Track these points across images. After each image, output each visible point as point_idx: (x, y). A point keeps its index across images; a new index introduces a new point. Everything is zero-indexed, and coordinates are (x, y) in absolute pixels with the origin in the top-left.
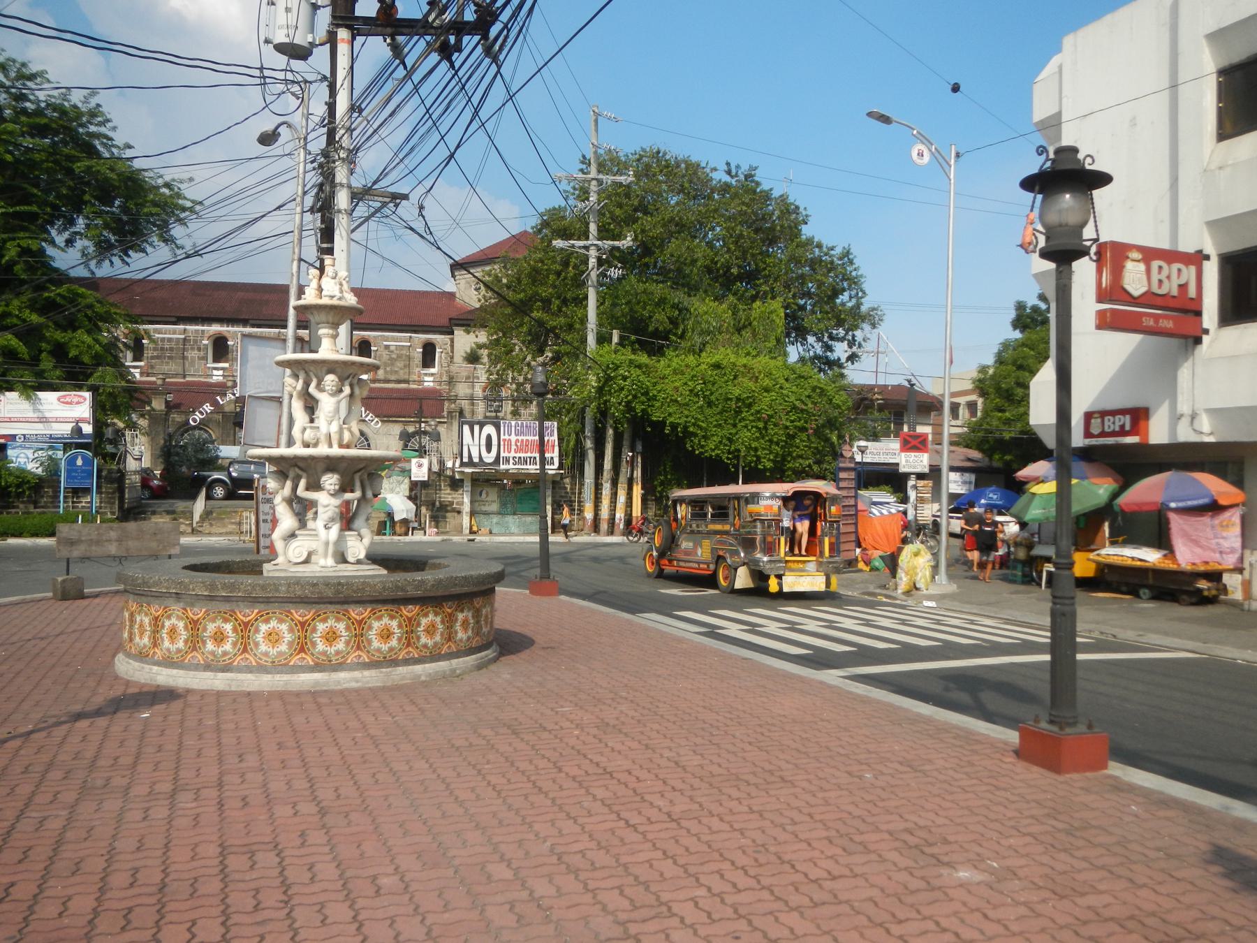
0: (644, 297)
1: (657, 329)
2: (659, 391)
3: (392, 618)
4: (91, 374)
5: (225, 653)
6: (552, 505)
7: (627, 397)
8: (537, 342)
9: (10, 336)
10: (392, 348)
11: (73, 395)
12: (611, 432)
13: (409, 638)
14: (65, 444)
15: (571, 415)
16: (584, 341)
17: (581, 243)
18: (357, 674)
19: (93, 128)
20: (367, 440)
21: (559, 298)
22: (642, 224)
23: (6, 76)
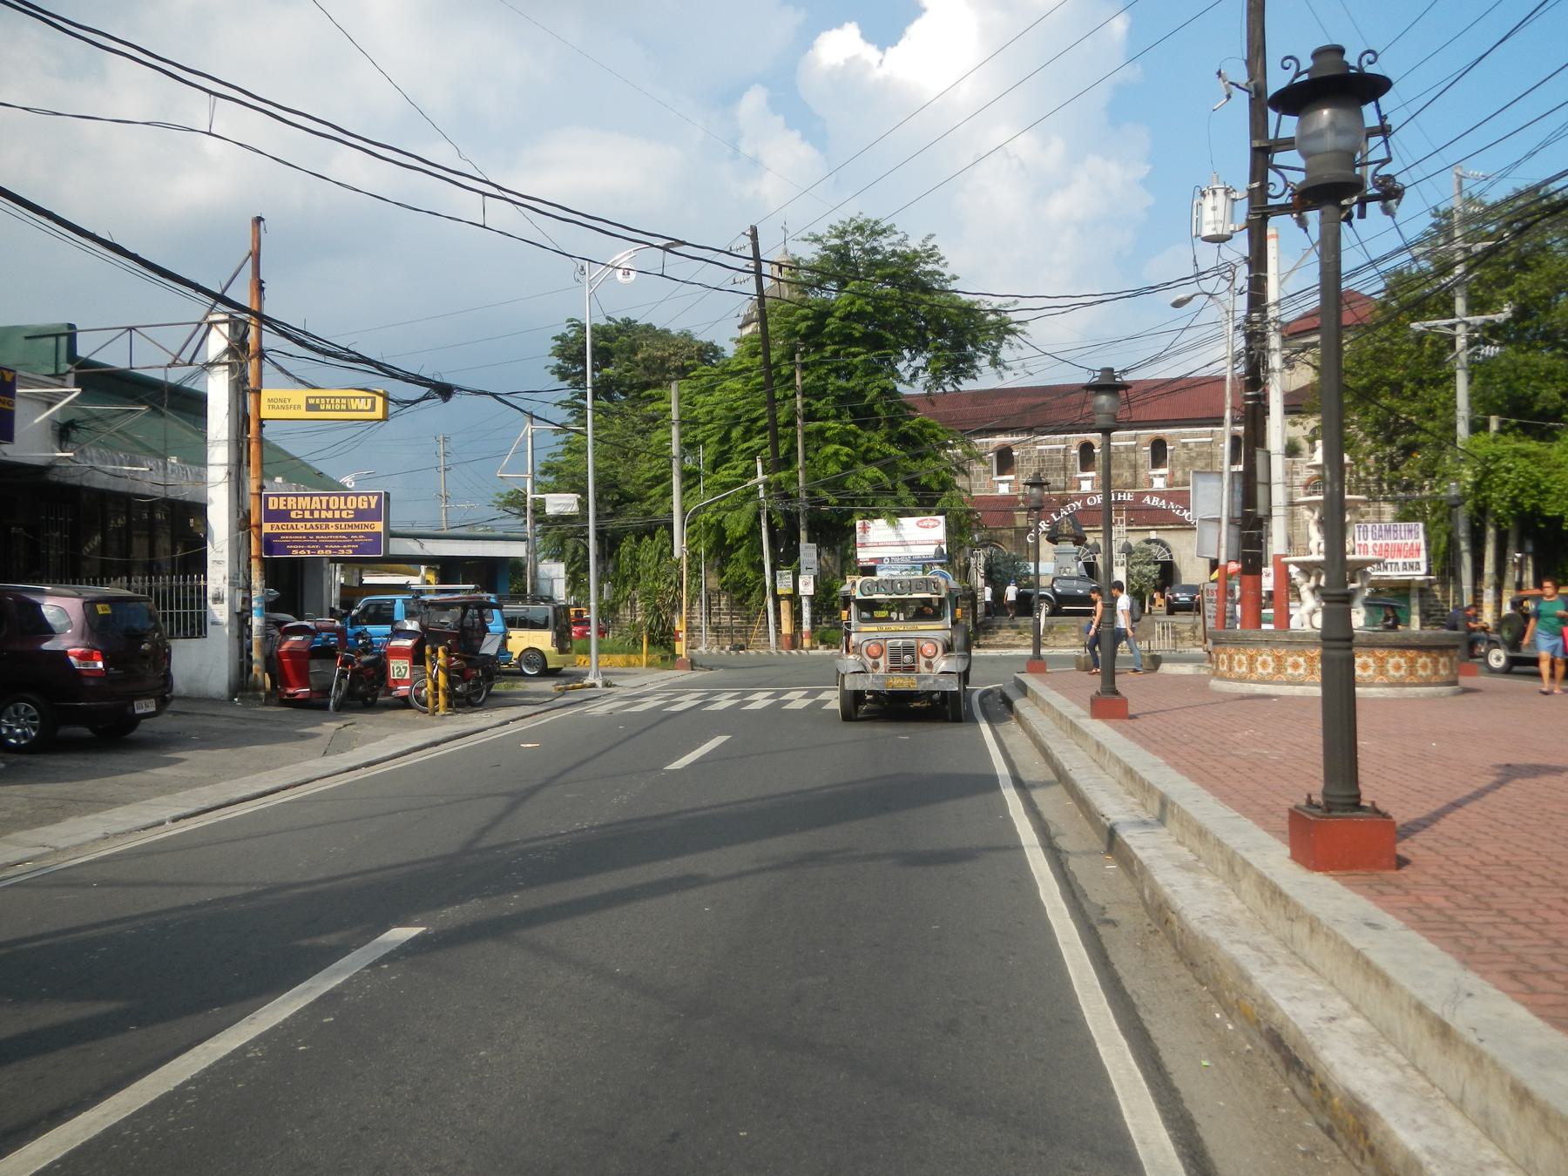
0: (1526, 371)
1: (1545, 408)
2: (1554, 483)
3: (1401, 657)
4: (938, 499)
5: (1300, 675)
6: (1420, 615)
7: (1512, 491)
8: (1387, 429)
9: (875, 469)
10: (1191, 446)
11: (929, 520)
12: (1491, 531)
13: (1412, 670)
14: (924, 565)
15: (1439, 514)
16: (1453, 427)
17: (1447, 322)
18: (1381, 690)
19: (929, 268)
20: (1169, 551)
21: (1411, 380)
22: (1521, 284)
23: (861, 235)
